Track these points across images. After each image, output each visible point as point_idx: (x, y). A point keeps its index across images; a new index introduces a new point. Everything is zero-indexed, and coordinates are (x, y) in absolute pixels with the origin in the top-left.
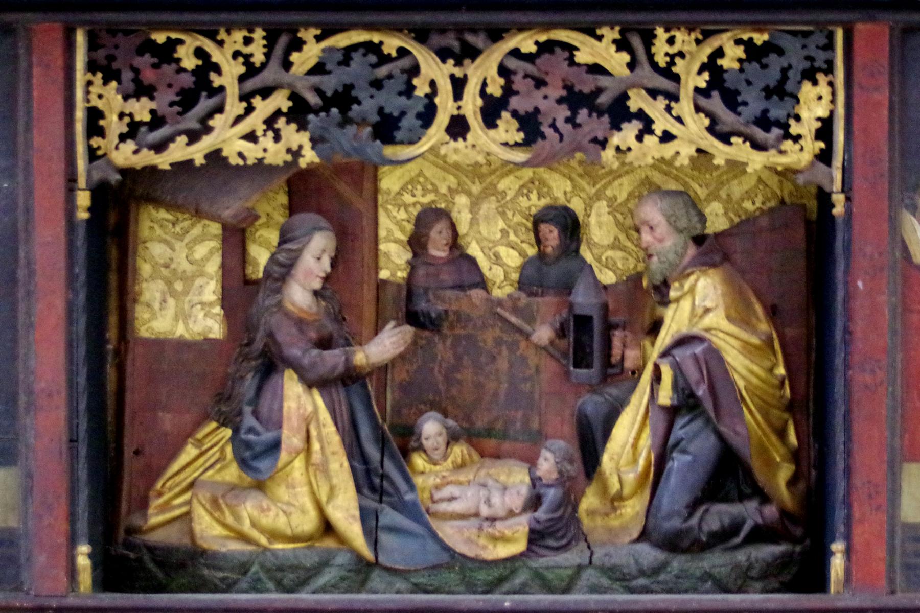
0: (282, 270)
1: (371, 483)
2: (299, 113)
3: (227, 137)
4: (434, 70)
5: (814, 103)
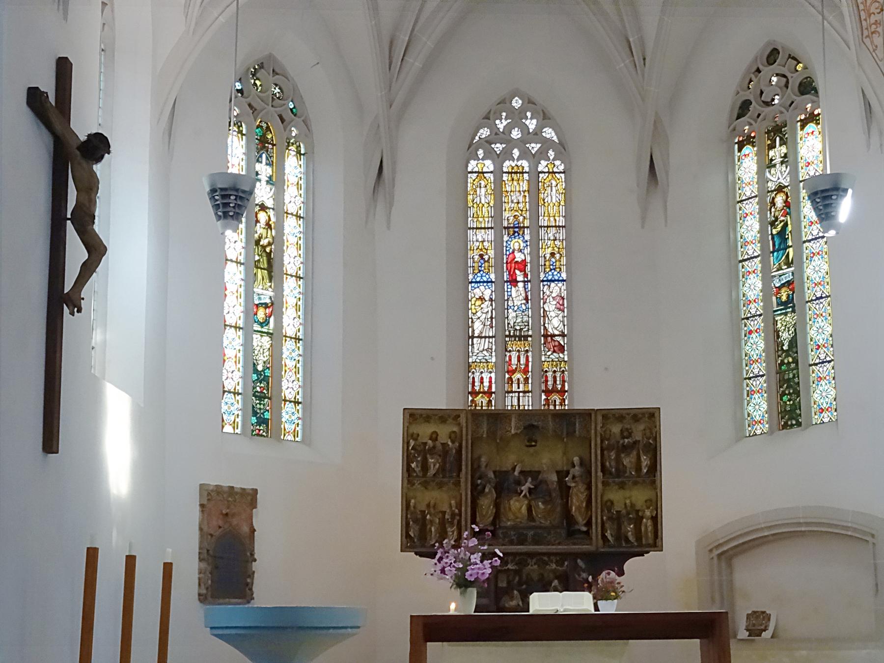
0: (513, 580)
1: (522, 600)
2: (516, 564)
3: (510, 566)
4: (529, 560)
5: (566, 563)
